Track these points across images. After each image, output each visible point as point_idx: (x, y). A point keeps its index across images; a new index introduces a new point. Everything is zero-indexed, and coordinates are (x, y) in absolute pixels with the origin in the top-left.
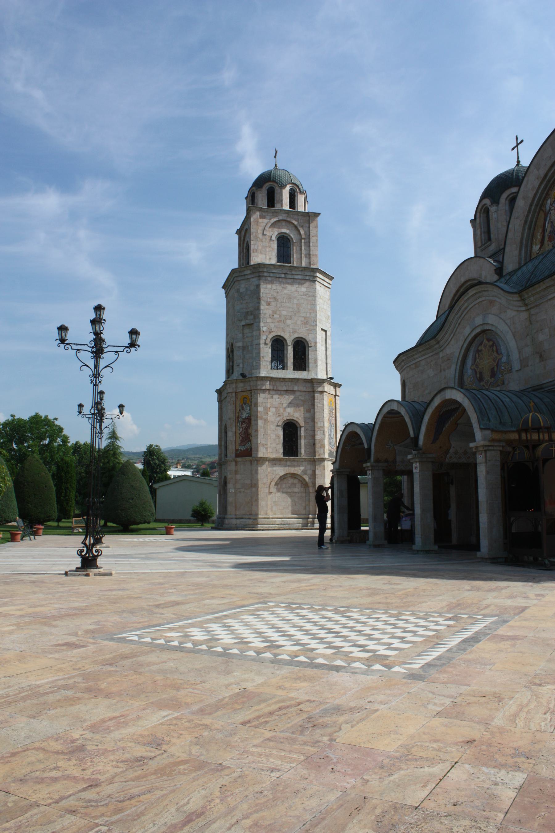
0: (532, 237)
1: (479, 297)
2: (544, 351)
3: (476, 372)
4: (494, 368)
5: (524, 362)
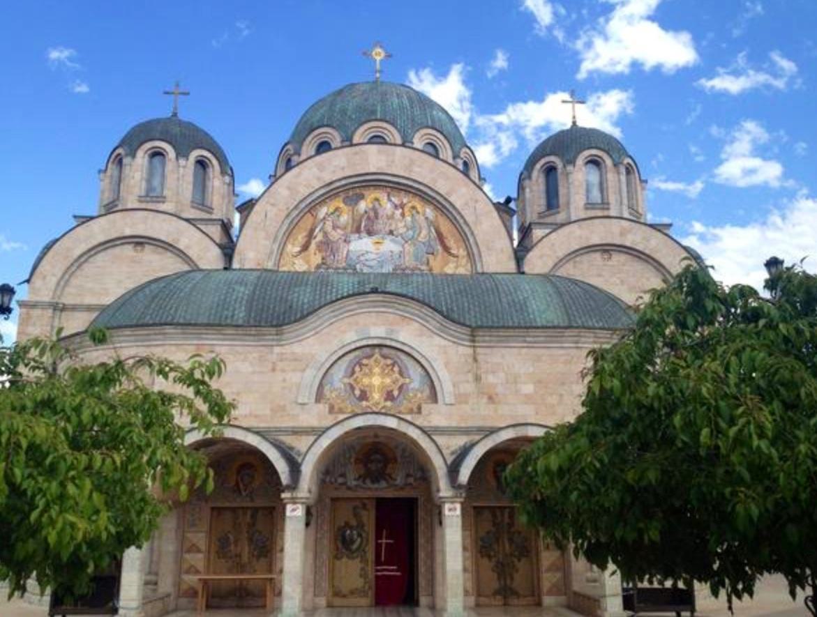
0: (289, 234)
1: (384, 306)
2: (497, 394)
3: (352, 388)
4: (392, 391)
5: (461, 399)
